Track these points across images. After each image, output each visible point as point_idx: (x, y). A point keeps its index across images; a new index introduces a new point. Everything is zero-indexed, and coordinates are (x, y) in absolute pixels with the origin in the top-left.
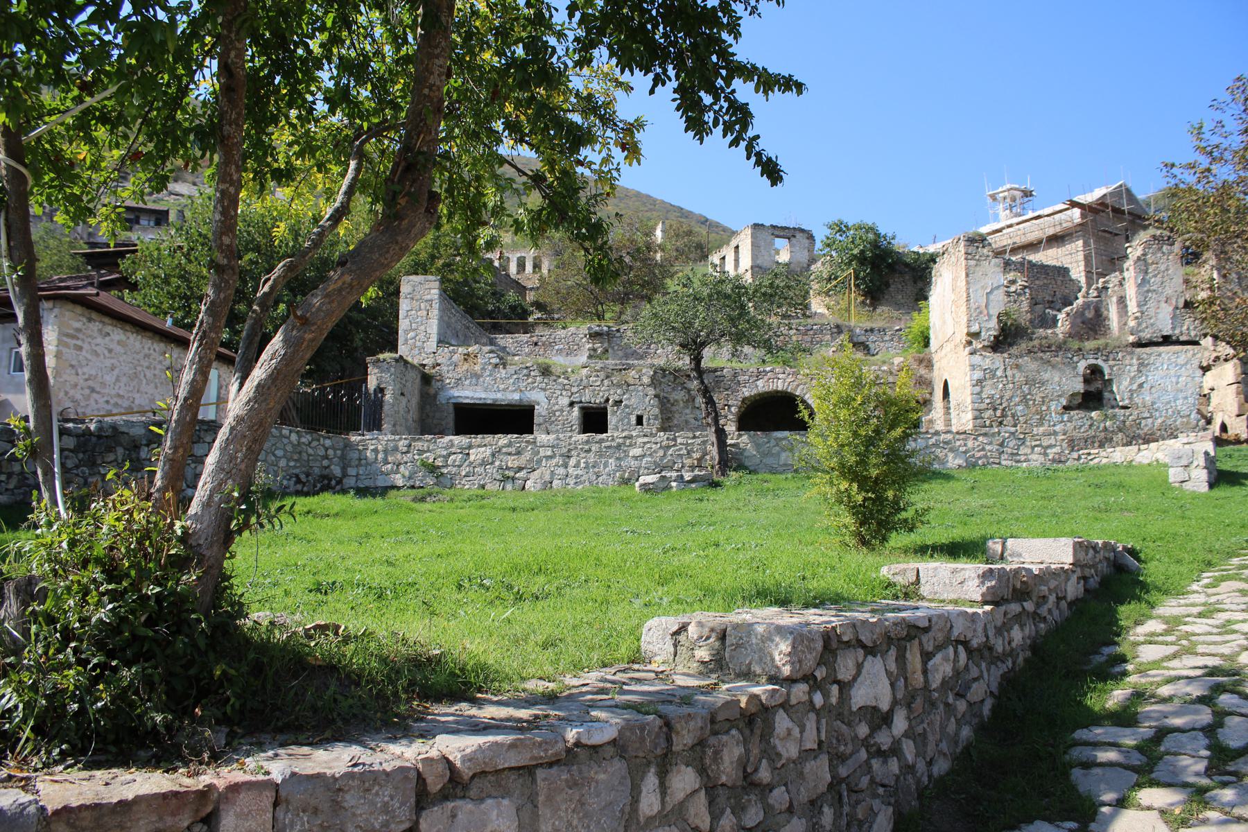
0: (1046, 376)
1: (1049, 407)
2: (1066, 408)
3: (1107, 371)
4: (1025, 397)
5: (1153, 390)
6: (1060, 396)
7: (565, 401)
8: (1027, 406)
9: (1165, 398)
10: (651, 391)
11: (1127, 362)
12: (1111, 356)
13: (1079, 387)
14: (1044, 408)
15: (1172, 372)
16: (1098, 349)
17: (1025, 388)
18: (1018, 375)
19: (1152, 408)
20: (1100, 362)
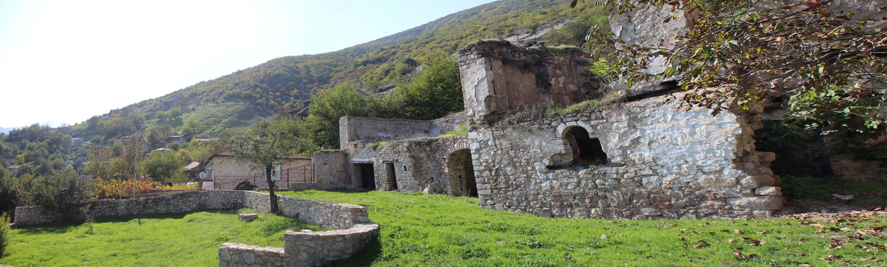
0: (527, 141)
1: (533, 168)
2: (551, 168)
3: (589, 130)
4: (512, 159)
5: (654, 145)
6: (542, 158)
7: (381, 161)
8: (515, 167)
9: (675, 153)
10: (407, 154)
11: (613, 119)
12: (593, 116)
13: (559, 147)
14: (529, 168)
15: (682, 122)
16: (577, 112)
17: (512, 153)
18: (504, 143)
19: (654, 166)
20: (581, 124)
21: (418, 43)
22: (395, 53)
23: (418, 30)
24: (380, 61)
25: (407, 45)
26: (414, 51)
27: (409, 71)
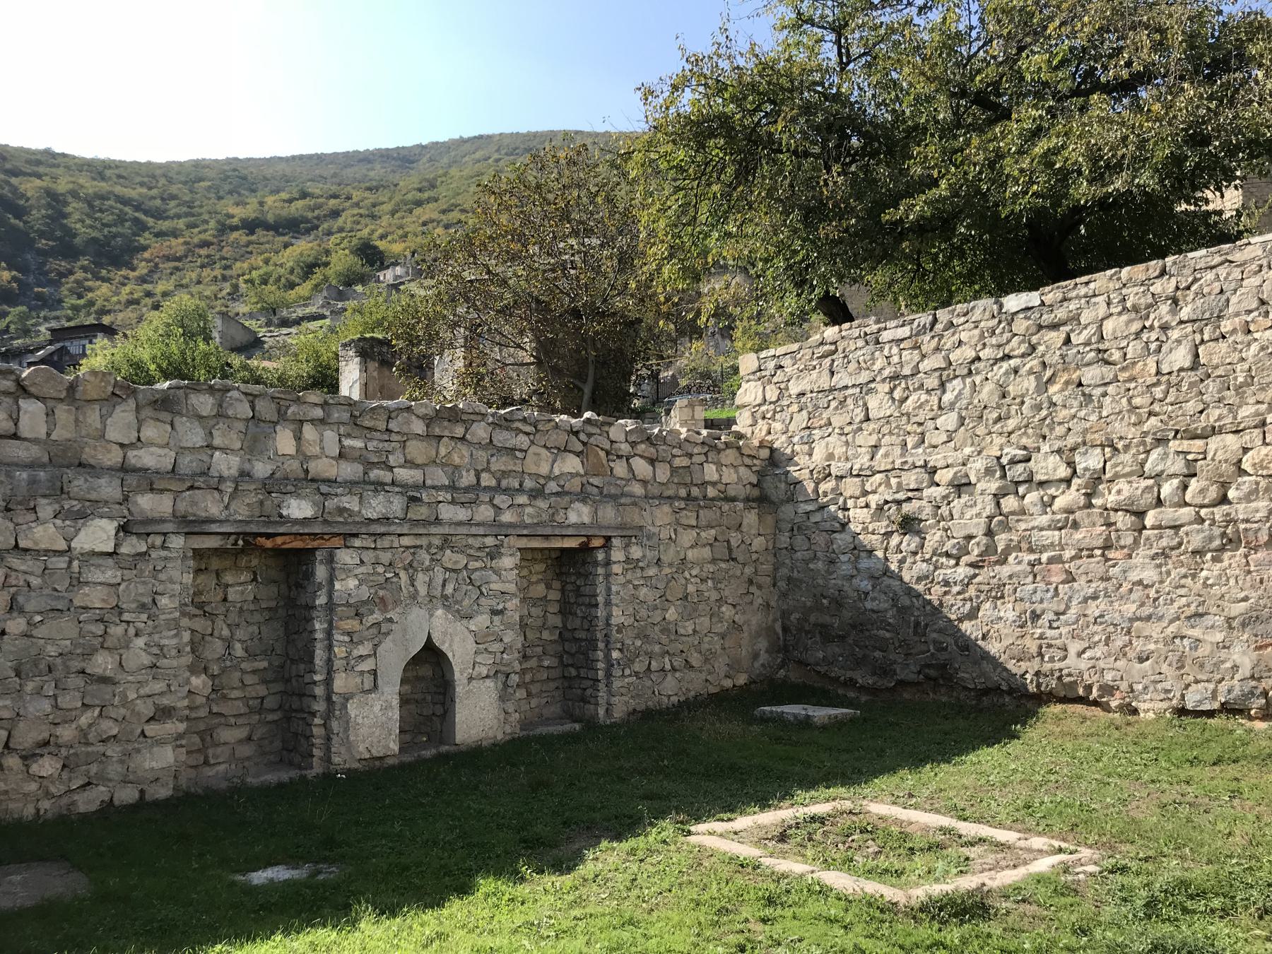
21: (398, 198)
22: (335, 214)
23: (403, 158)
24: (293, 227)
25: (371, 198)
26: (385, 220)
27: (362, 279)
